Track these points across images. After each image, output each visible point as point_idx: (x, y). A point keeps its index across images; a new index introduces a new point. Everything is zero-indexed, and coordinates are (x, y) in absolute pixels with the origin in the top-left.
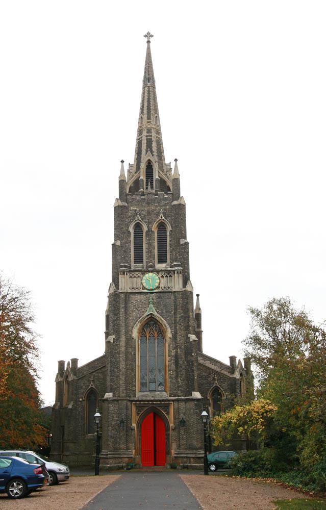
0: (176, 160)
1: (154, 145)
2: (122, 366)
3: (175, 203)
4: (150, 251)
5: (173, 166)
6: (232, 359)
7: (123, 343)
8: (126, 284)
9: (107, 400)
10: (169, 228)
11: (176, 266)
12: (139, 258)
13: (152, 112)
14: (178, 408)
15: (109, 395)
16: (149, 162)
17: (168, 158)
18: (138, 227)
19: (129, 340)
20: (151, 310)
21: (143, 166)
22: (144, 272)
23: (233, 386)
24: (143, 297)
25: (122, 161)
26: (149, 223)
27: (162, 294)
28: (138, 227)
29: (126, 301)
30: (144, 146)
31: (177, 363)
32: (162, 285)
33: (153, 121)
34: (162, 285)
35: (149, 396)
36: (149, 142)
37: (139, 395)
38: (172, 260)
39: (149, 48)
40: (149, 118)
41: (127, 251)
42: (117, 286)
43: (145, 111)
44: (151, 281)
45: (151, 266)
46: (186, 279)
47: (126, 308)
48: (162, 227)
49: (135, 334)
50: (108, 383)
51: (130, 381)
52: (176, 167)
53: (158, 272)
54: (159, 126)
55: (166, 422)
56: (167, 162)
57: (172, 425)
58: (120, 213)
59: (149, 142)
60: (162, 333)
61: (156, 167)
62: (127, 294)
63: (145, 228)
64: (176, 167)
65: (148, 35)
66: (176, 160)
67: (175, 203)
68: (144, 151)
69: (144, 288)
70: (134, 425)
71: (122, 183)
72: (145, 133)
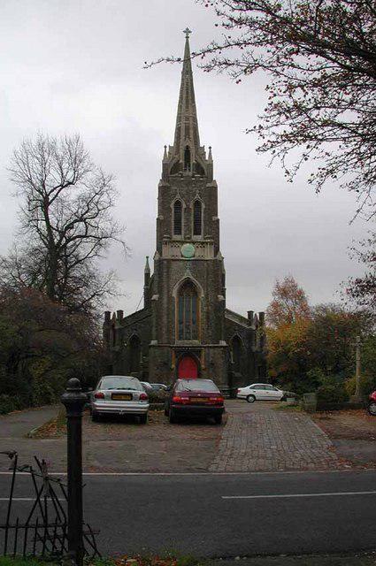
0: (210, 148)
1: (191, 131)
2: (165, 319)
3: (209, 185)
4: (187, 226)
5: (207, 150)
6: (250, 313)
7: (165, 300)
8: (169, 252)
9: (154, 346)
10: (203, 206)
11: (209, 238)
12: (178, 231)
13: (190, 102)
14: (208, 354)
15: (153, 342)
16: (187, 147)
17: (204, 141)
18: (178, 204)
19: (170, 298)
20: (188, 274)
21: (182, 152)
22: (183, 243)
23: (250, 335)
24: (181, 263)
25: (165, 147)
26: (187, 201)
27: (196, 262)
28: (178, 204)
29: (168, 268)
30: (183, 133)
31: (208, 318)
32: (197, 254)
33: (191, 111)
34: (197, 254)
35: (186, 343)
36: (187, 129)
37: (178, 343)
38: (205, 234)
39: (187, 43)
40: (187, 107)
41: (168, 225)
42: (161, 254)
43: (184, 101)
44: (188, 250)
45: (189, 238)
46: (217, 250)
47: (168, 272)
48: (197, 204)
49: (174, 294)
50: (154, 333)
51: (169, 332)
52: (210, 154)
53: (194, 243)
54: (195, 115)
55: (198, 364)
56: (201, 145)
57: (203, 366)
58: (164, 192)
59: (187, 134)
60: (196, 294)
61: (193, 152)
62: (168, 260)
63: (184, 206)
64: (210, 154)
65: (187, 31)
66: (210, 148)
67: (209, 185)
68: (183, 137)
69: (182, 256)
70: (173, 366)
71: (165, 166)
72: (183, 121)
